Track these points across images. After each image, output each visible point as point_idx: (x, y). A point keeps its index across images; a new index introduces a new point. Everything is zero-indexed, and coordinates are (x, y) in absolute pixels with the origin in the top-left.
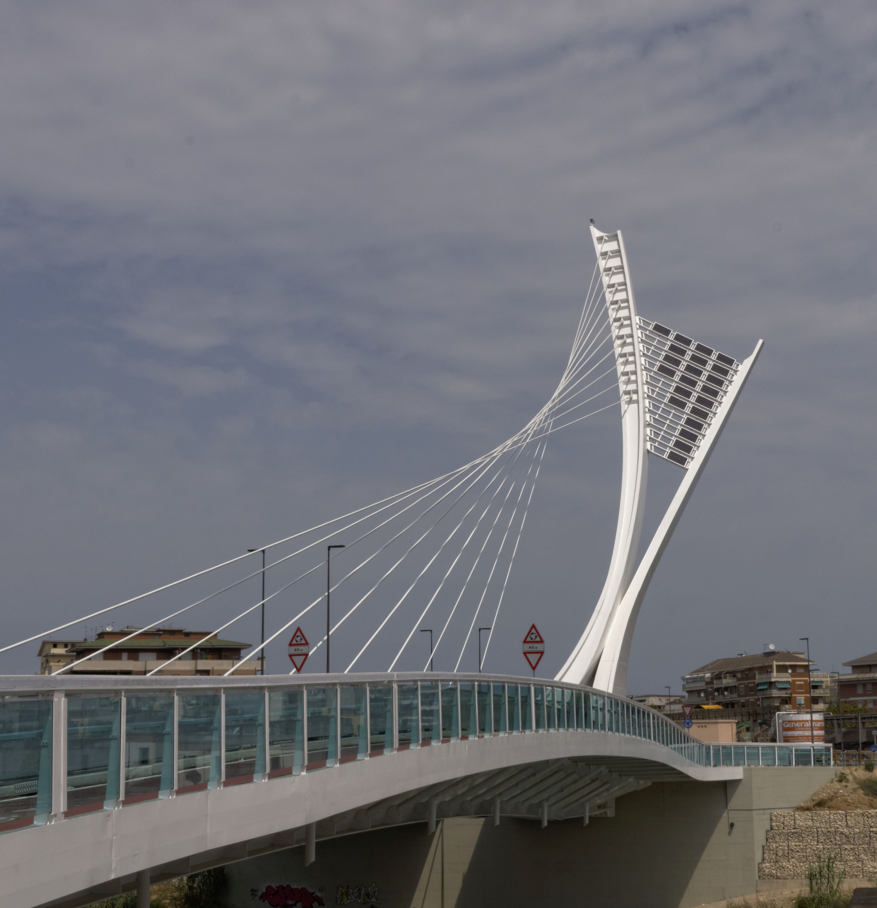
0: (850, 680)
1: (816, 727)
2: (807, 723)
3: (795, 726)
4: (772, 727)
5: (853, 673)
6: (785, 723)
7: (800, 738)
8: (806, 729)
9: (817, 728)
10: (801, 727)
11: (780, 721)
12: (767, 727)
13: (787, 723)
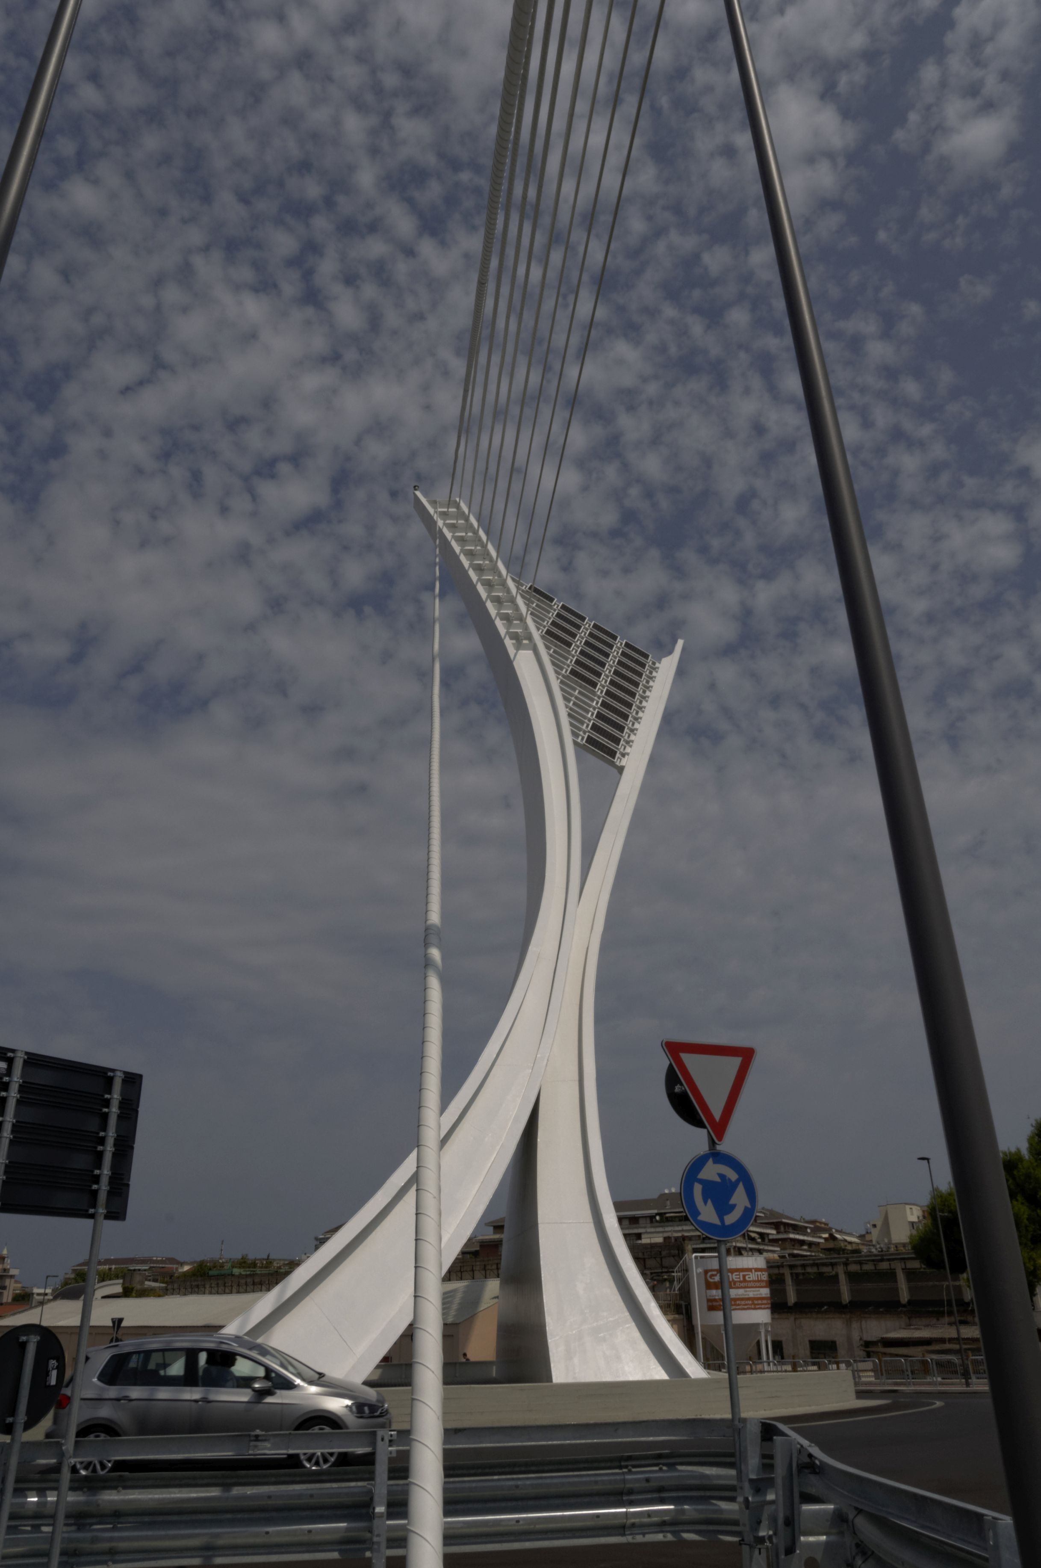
0: (493, 1240)
1: (762, 1281)
2: (750, 1273)
3: (731, 1280)
4: (675, 1282)
5: (495, 1233)
6: (710, 1273)
7: (738, 1302)
8: (750, 1285)
9: (764, 1284)
10: (740, 1282)
11: (700, 1270)
12: (655, 1282)
13: (714, 1273)
